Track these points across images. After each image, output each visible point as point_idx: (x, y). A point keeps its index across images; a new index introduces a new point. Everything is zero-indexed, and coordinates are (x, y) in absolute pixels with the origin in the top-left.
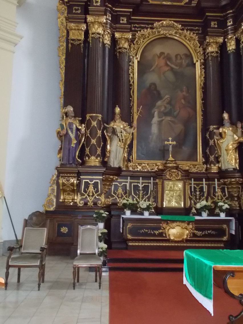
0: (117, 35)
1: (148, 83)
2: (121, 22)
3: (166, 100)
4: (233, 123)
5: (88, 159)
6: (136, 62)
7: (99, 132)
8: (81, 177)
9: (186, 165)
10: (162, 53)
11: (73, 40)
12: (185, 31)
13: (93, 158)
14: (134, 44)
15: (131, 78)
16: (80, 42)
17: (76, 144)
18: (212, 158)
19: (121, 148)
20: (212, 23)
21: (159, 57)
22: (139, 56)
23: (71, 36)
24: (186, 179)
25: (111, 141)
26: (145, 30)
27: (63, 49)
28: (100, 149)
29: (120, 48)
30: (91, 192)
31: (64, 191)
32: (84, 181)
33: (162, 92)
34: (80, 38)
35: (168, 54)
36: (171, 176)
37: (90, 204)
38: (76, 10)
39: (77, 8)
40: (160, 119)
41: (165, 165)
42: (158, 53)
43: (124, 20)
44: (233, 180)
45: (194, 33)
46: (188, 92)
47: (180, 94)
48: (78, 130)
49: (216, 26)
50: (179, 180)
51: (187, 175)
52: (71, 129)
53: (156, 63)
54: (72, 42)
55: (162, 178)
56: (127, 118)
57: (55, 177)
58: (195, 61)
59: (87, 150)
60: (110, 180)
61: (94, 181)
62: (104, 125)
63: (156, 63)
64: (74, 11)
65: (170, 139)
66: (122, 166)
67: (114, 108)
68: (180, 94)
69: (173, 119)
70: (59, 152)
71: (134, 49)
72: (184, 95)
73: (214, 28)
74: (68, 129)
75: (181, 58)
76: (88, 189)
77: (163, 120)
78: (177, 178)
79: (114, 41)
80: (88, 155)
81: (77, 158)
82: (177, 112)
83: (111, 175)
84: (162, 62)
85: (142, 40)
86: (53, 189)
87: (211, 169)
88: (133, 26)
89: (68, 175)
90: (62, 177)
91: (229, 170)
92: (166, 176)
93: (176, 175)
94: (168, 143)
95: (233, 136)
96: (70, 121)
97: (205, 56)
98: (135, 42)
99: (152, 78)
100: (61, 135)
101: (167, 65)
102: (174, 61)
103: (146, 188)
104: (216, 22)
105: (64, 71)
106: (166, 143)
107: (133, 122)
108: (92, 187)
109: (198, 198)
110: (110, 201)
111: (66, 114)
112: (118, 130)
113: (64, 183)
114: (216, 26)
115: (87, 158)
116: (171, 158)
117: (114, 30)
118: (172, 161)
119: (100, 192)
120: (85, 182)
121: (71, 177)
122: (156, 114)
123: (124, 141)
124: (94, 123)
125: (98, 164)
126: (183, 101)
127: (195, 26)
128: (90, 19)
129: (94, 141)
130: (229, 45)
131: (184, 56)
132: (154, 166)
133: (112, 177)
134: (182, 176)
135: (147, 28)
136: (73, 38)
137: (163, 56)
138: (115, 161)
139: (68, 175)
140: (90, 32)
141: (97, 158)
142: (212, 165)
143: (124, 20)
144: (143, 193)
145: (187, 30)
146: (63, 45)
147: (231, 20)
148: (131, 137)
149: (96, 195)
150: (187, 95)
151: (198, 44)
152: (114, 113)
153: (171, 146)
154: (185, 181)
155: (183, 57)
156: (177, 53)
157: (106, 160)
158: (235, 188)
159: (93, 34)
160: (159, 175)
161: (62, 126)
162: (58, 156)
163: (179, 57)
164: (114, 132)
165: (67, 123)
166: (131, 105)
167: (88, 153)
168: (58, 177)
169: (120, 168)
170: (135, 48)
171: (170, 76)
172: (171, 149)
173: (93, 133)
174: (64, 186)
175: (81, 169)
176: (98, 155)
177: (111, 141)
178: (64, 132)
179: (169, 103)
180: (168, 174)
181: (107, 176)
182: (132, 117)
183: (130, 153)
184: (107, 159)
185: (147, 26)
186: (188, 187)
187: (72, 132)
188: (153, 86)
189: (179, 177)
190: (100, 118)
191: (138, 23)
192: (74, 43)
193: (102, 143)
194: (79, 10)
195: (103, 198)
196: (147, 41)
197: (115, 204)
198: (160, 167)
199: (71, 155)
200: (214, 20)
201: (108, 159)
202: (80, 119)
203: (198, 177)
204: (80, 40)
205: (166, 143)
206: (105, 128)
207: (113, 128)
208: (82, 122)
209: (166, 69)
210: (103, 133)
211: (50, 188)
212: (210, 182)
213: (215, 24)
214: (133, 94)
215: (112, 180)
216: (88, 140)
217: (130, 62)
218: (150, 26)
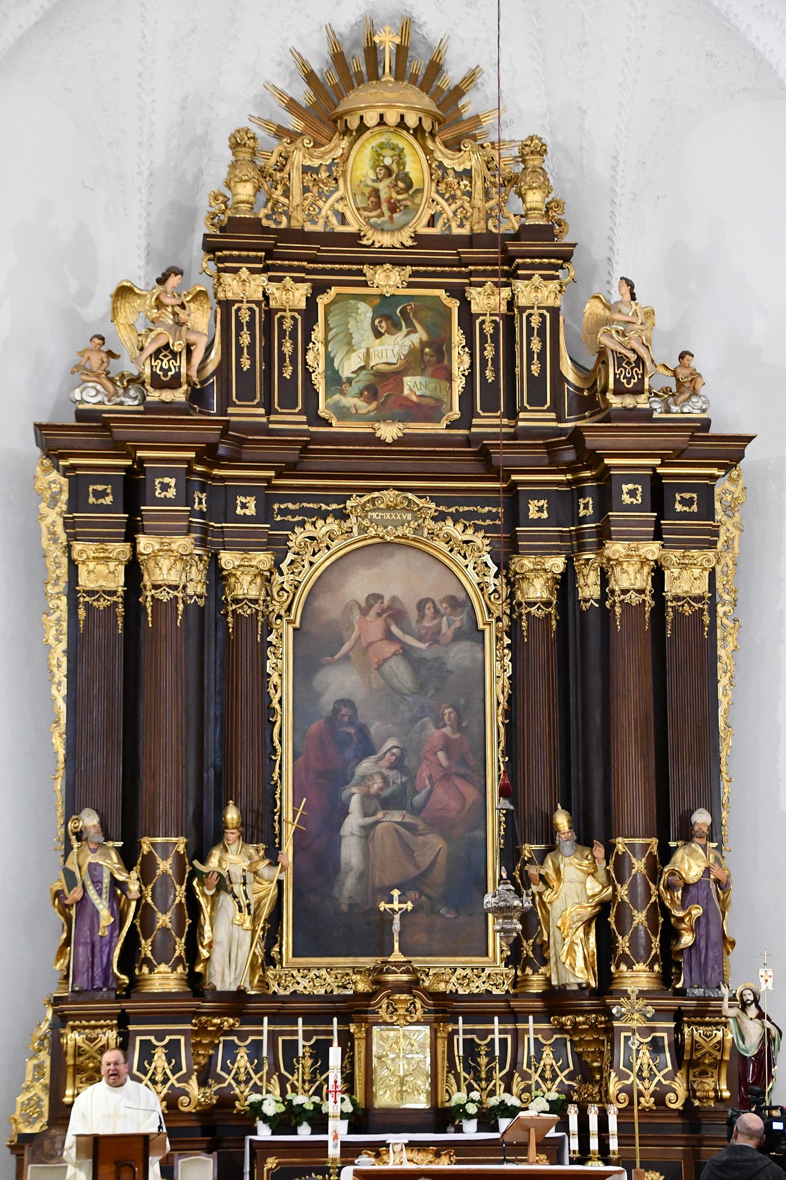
0: (228, 559)
1: (327, 702)
2: (239, 511)
3: (388, 755)
4: (584, 839)
5: (150, 973)
7: (181, 891)
8: (131, 1028)
11: (91, 593)
12: (450, 522)
13: (163, 967)
14: (281, 574)
15: (275, 686)
16: (115, 599)
17: (112, 927)
18: (527, 948)
19: (242, 932)
20: (533, 505)
21: (364, 612)
23: (85, 581)
24: (437, 1021)
26: (320, 523)
27: (59, 620)
28: (183, 940)
29: (236, 601)
30: (159, 1070)
32: (138, 1039)
33: (375, 728)
34: (112, 586)
35: (394, 599)
36: (392, 1013)
38: (99, 495)
39: (100, 488)
40: (370, 820)
41: (376, 975)
42: (362, 598)
44: (580, 1019)
45: (477, 529)
46: (458, 728)
47: (434, 734)
48: (115, 882)
49: (545, 515)
50: (418, 1023)
52: (97, 882)
53: (354, 636)
54: (87, 599)
55: (367, 1018)
57: (45, 1027)
58: (481, 626)
59: (146, 948)
60: (211, 1031)
61: (168, 1038)
62: (191, 865)
63: (354, 636)
64: (92, 500)
65: (396, 893)
66: (247, 986)
67: (221, 809)
68: (434, 734)
69: (408, 819)
70: (61, 953)
71: (282, 589)
72: (445, 736)
73: (539, 522)
74: (88, 882)
75: (437, 612)
76: (150, 1064)
77: (377, 822)
78: (412, 1017)
80: (146, 961)
81: (116, 970)
82: (424, 793)
83: (215, 1015)
84: (374, 628)
85: (308, 557)
86: (39, 1067)
87: (526, 980)
88: (279, 508)
89: (93, 1023)
90: (73, 1028)
91: (568, 988)
92: (378, 1013)
93: (407, 1010)
94: (388, 906)
95: (584, 883)
97: (512, 610)
98: (284, 566)
100: (67, 902)
101: (389, 636)
102: (414, 624)
104: (543, 502)
105: (64, 691)
106: (383, 906)
107: (280, 848)
108: (164, 1057)
109: (483, 1075)
111: (79, 836)
112: (237, 876)
113: (80, 1047)
114: (545, 515)
115: (145, 970)
116: (397, 956)
118: (397, 964)
119: (184, 1070)
120: (141, 1041)
121: (102, 1027)
122: (355, 804)
123: (252, 908)
124: (165, 866)
126: (441, 755)
127: (484, 503)
129: (164, 919)
130: (581, 582)
131: (444, 605)
132: (347, 974)
133: (217, 1021)
134: (425, 1013)
135: (324, 515)
136: (92, 586)
137: (376, 608)
138: (227, 972)
139: (93, 1023)
140: (147, 580)
141: (174, 969)
142: (529, 971)
143: (249, 506)
144: (312, 1065)
146: (58, 607)
147: (589, 500)
148: (274, 892)
149: (173, 1080)
150: (456, 736)
151: (490, 563)
153: (397, 917)
154: (435, 1025)
155: (443, 607)
156: (424, 596)
157: (199, 969)
158: (589, 1043)
159: (156, 587)
161: (70, 876)
162: (58, 967)
163: (429, 611)
164: (223, 884)
165: (85, 868)
166: (276, 776)
167: (149, 955)
170: (285, 586)
172: (396, 926)
174: (80, 1055)
176: (179, 960)
178: (76, 894)
179: (397, 765)
180: (384, 1006)
181: (204, 1019)
182: (276, 818)
183: (272, 936)
184: (202, 965)
185: (324, 507)
186: (442, 1046)
187: (100, 893)
188: (344, 710)
189: (419, 1014)
190: (181, 849)
191: (294, 499)
192: (95, 604)
193: (188, 921)
194: (108, 495)
195: (193, 1086)
196: (323, 560)
198: (362, 987)
199: (97, 961)
200: (537, 496)
201: (205, 967)
202: (120, 844)
204: (113, 593)
205: (382, 909)
206: (194, 873)
207: (220, 874)
208: (128, 857)
209: (389, 649)
210: (190, 891)
211: (31, 1064)
212: (520, 1026)
213: (540, 509)
214: (280, 742)
216: (145, 913)
217: (270, 632)
218: (334, 506)
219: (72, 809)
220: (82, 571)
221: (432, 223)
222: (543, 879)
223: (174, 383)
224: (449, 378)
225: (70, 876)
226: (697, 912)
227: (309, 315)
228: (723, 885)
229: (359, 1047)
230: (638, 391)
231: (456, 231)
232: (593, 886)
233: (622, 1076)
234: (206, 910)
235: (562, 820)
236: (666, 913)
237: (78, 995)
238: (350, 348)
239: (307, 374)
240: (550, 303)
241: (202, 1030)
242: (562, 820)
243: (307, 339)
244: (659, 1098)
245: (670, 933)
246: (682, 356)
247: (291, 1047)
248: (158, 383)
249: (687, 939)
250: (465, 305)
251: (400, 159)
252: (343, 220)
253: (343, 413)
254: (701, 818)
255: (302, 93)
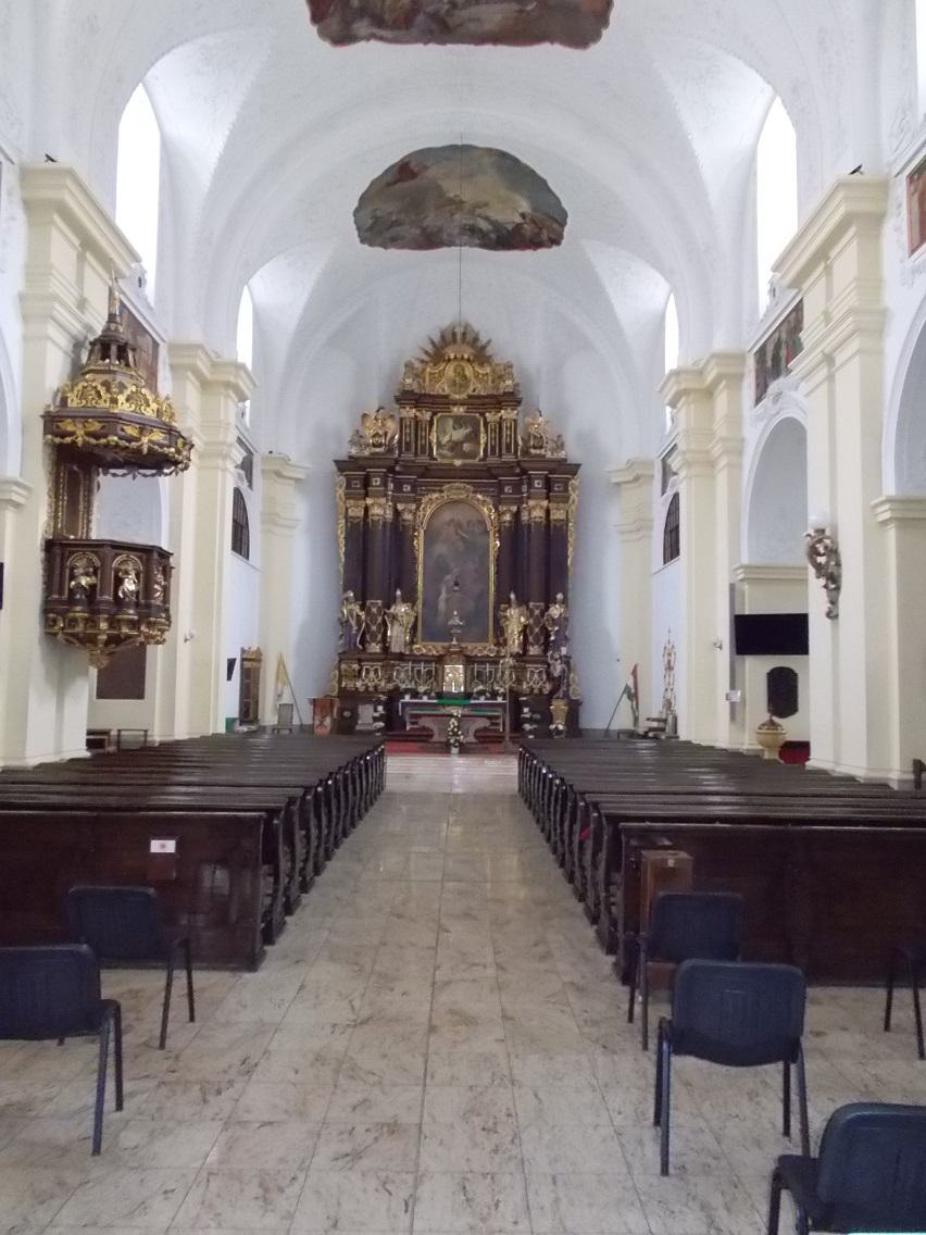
0: (400, 507)
6: (422, 531)
7: (380, 619)
9: (475, 648)
10: (453, 520)
22: (425, 525)
23: (350, 513)
25: (392, 625)
29: (403, 520)
31: (346, 676)
37: (371, 689)
43: (407, 488)
48: (358, 616)
51: (469, 661)
52: (352, 616)
56: (410, 598)
59: (368, 636)
79: (397, 513)
84: (452, 530)
86: (335, 676)
96: (350, 607)
99: (440, 549)
103: (429, 672)
110: (390, 686)
111: (347, 599)
116: (454, 642)
117: (395, 501)
122: (444, 590)
124: (374, 610)
125: (378, 651)
127: (490, 487)
128: (369, 501)
129: (374, 628)
135: (435, 491)
143: (407, 488)
145: (481, 493)
148: (413, 619)
152: (395, 597)
160: (440, 660)
164: (394, 617)
168: (340, 661)
169: (401, 654)
171: (460, 545)
173: (374, 620)
175: (362, 656)
177: (392, 625)
178: (344, 620)
186: (469, 672)
195: (383, 684)
197: (397, 688)
200: (509, 484)
203: (483, 661)
206: (385, 613)
208: (363, 607)
209: (457, 537)
215: (394, 666)
216: (367, 625)
219: (345, 590)
220: (350, 510)
221: (474, 390)
222: (505, 617)
223: (380, 445)
224: (479, 444)
225: (343, 613)
226: (556, 628)
227: (431, 423)
228: (566, 619)
229: (440, 673)
230: (541, 447)
231: (482, 393)
232: (523, 619)
233: (528, 683)
234: (389, 625)
235: (512, 596)
236: (546, 629)
237: (344, 652)
238: (445, 433)
239: (430, 443)
240: (514, 417)
241: (387, 665)
242: (512, 596)
243: (430, 431)
244: (540, 690)
245: (548, 635)
246: (559, 436)
247: (419, 671)
248: (374, 445)
249: (552, 638)
250: (485, 419)
251: (463, 370)
252: (444, 390)
253: (443, 456)
254: (560, 596)
255: (430, 348)
